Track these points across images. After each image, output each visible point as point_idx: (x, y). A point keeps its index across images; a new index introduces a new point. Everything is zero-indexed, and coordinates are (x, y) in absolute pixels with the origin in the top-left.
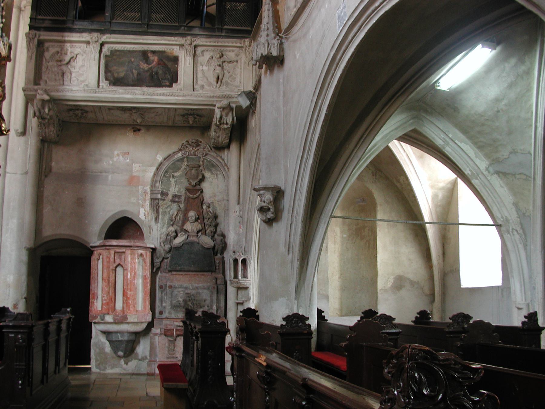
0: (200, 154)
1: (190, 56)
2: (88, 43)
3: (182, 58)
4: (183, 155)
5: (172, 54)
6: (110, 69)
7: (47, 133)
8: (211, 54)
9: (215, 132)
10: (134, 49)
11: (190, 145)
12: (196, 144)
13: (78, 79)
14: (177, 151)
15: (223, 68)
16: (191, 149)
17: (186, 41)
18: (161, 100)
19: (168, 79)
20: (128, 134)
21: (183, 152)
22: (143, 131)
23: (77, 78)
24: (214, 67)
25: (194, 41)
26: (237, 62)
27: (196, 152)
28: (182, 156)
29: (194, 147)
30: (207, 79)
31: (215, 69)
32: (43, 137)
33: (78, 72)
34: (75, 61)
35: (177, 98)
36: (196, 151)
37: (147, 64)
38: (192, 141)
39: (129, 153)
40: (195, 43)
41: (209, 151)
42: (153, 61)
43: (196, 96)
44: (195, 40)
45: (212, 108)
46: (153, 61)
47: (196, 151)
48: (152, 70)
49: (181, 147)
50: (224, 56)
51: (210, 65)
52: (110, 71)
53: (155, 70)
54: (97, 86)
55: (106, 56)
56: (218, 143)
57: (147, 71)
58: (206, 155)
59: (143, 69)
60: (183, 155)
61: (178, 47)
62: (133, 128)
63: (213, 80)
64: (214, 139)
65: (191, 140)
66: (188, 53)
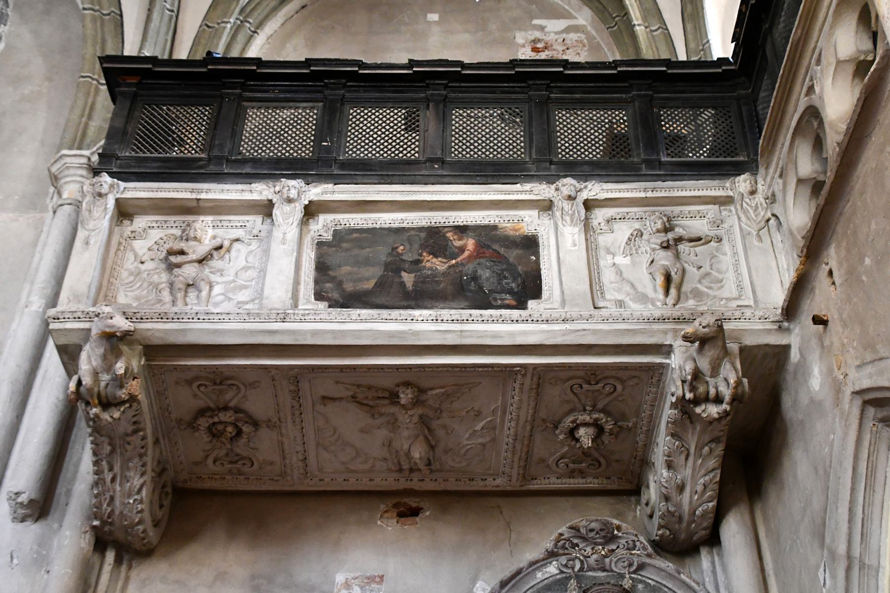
0: (620, 564)
1: (575, 225)
2: (266, 209)
3: (548, 238)
4: (565, 570)
5: (516, 230)
6: (331, 273)
7: (117, 502)
8: (637, 225)
9: (670, 466)
10: (405, 225)
11: (584, 539)
12: (603, 534)
13: (230, 299)
14: (543, 560)
15: (677, 256)
16: (589, 549)
17: (557, 189)
18: (495, 335)
19: (512, 289)
20: (379, 523)
21: (563, 560)
22: (428, 513)
23: (230, 295)
24: (649, 255)
25: (580, 190)
26: (720, 240)
27: (607, 560)
28: (562, 572)
29: (597, 544)
30: (632, 285)
31: (652, 262)
32: (104, 523)
33: (234, 281)
34: (227, 256)
35: (545, 327)
36: (605, 556)
37: (445, 257)
38: (589, 528)
39: (382, 577)
40: (585, 195)
41: (649, 556)
42: (462, 250)
43: (605, 320)
44: (586, 187)
45: (658, 360)
46: (462, 250)
47: (605, 556)
48: (461, 271)
49: (556, 545)
50: (677, 230)
51: (636, 250)
52: (333, 279)
53: (470, 268)
54: (289, 302)
55: (320, 244)
56: (680, 519)
57: (444, 274)
58: (641, 567)
59: (431, 269)
60: (565, 570)
61: (535, 213)
62: (395, 506)
63: (652, 288)
64: (667, 499)
65: (584, 523)
66: (568, 218)
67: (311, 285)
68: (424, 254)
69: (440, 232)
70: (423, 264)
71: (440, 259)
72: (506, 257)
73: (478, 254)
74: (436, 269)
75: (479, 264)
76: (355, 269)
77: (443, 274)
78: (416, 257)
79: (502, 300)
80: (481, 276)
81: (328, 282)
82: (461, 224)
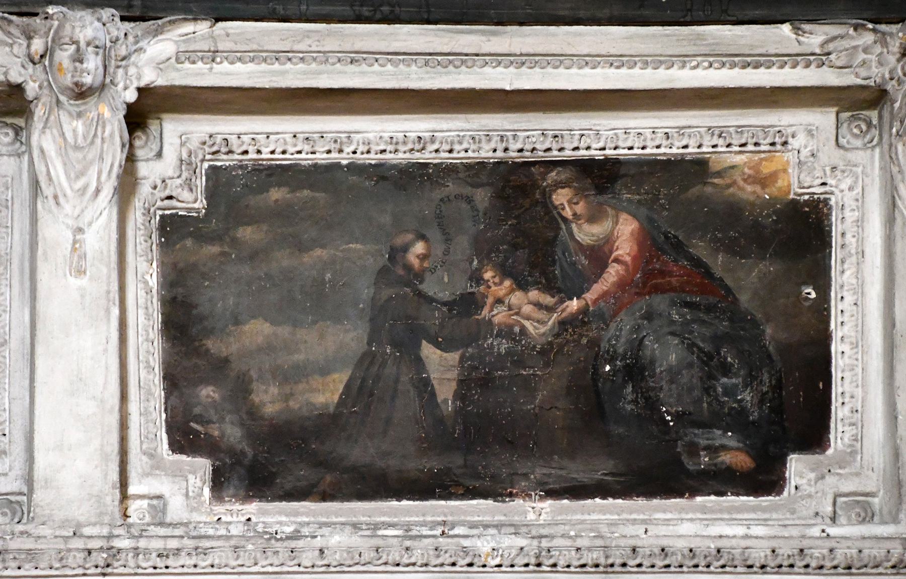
3: (860, 223)
5: (764, 181)
6: (212, 345)
10: (427, 157)
19: (742, 412)
37: (549, 287)
48: (594, 343)
59: (506, 332)
67: (159, 392)
68: (488, 275)
69: (535, 186)
70: (485, 312)
71: (534, 294)
72: (729, 290)
73: (649, 275)
74: (523, 330)
75: (649, 316)
76: (284, 331)
77: (543, 352)
78: (463, 286)
79: (713, 450)
80: (652, 362)
81: (205, 381)
82: (598, 155)
